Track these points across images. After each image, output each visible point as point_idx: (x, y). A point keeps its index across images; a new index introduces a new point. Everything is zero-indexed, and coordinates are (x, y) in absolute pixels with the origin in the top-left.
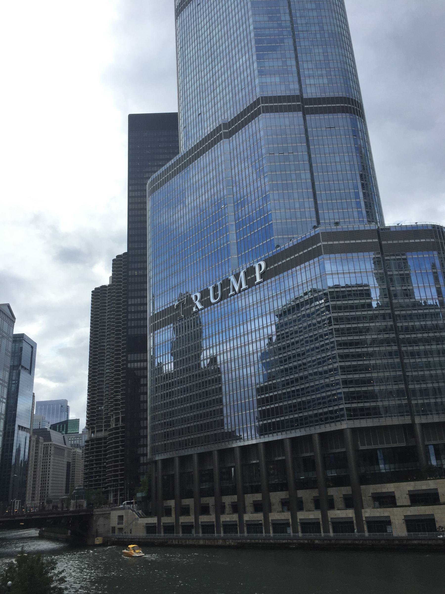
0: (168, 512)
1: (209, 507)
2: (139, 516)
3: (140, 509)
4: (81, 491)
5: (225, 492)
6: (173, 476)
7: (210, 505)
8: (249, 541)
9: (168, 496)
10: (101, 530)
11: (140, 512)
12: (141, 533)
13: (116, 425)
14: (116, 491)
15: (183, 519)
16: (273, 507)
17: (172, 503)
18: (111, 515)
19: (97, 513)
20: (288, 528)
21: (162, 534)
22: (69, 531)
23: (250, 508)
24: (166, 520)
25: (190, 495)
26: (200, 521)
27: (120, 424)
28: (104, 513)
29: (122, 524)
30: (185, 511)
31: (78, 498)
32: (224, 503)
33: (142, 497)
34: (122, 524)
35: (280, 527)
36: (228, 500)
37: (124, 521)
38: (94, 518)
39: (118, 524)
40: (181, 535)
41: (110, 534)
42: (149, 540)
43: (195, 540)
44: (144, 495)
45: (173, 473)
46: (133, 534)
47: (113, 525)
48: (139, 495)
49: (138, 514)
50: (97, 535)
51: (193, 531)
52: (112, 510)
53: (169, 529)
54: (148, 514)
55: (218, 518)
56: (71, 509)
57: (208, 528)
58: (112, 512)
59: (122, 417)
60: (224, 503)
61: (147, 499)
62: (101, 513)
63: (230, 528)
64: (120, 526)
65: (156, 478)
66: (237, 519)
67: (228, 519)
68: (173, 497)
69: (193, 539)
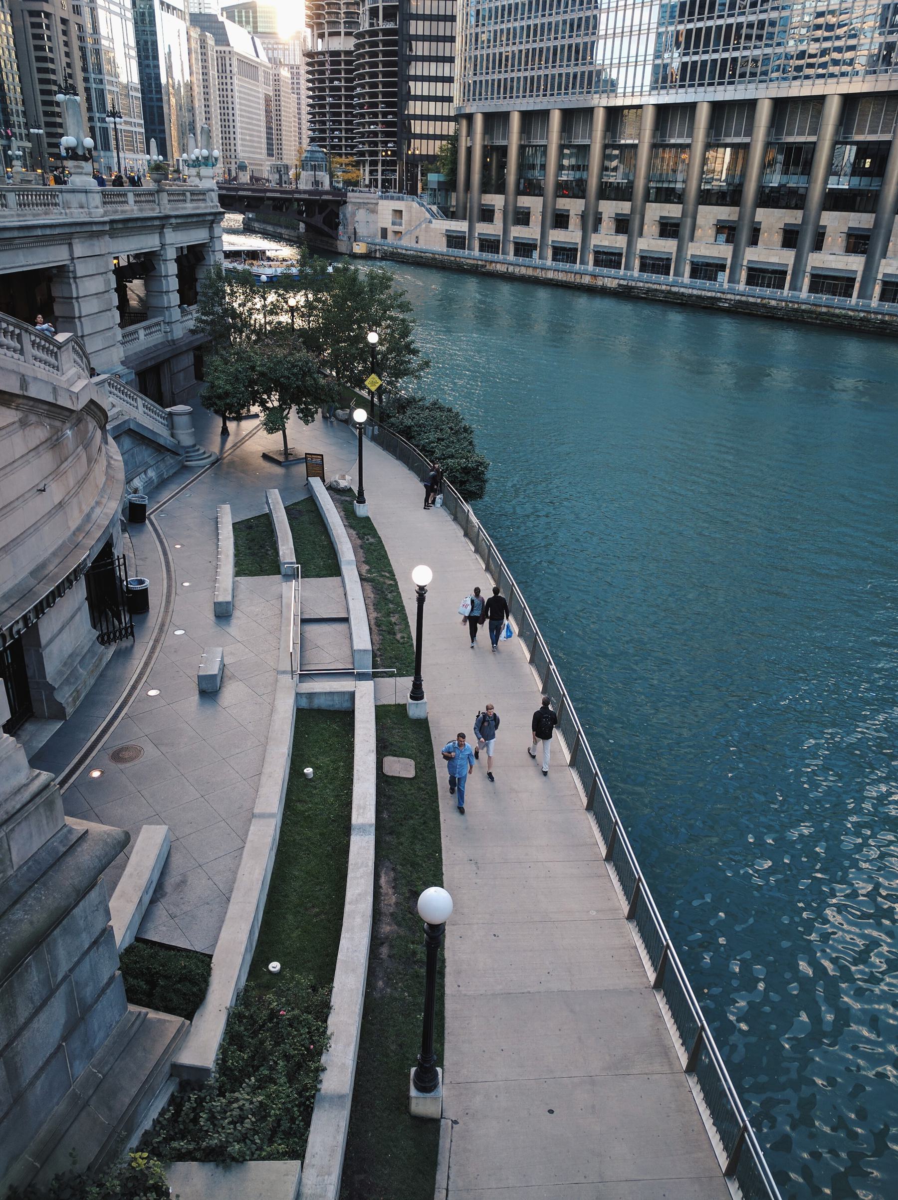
0: (487, 215)
1: (568, 216)
2: (432, 216)
3: (434, 204)
4: (317, 155)
5: (607, 192)
6: (503, 151)
7: (572, 213)
8: (641, 284)
9: (486, 188)
10: (362, 231)
11: (434, 208)
12: (438, 246)
13: (371, 25)
14: (374, 163)
15: (518, 232)
16: (698, 233)
17: (497, 201)
18: (380, 208)
19: (353, 200)
20: (720, 274)
21: (476, 253)
22: (302, 226)
23: (651, 228)
24: (482, 228)
25: (532, 188)
26: (550, 239)
27: (380, 22)
28: (366, 201)
29: (401, 225)
30: (523, 218)
31: (314, 168)
32: (601, 213)
33: (439, 182)
34: (401, 225)
35: (705, 270)
36: (609, 208)
37: (403, 221)
38: (349, 208)
39: (393, 224)
40: (511, 257)
41: (378, 240)
42: (453, 259)
43: (538, 270)
44: (442, 179)
45: (504, 143)
46: (422, 245)
47: (384, 226)
48: (433, 178)
49: (429, 211)
50: (355, 237)
51: (536, 254)
52: (381, 198)
53: (490, 245)
54: (449, 214)
55: (585, 239)
56: (302, 187)
57: (564, 253)
58: (381, 202)
59: (384, 7)
60: (601, 213)
61: (449, 186)
62: (361, 201)
63: (608, 259)
64: (397, 228)
65: (469, 150)
66: (624, 246)
67: (606, 243)
68: (501, 189)
69: (535, 268)
